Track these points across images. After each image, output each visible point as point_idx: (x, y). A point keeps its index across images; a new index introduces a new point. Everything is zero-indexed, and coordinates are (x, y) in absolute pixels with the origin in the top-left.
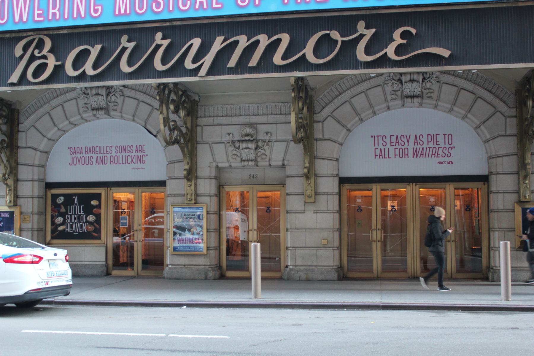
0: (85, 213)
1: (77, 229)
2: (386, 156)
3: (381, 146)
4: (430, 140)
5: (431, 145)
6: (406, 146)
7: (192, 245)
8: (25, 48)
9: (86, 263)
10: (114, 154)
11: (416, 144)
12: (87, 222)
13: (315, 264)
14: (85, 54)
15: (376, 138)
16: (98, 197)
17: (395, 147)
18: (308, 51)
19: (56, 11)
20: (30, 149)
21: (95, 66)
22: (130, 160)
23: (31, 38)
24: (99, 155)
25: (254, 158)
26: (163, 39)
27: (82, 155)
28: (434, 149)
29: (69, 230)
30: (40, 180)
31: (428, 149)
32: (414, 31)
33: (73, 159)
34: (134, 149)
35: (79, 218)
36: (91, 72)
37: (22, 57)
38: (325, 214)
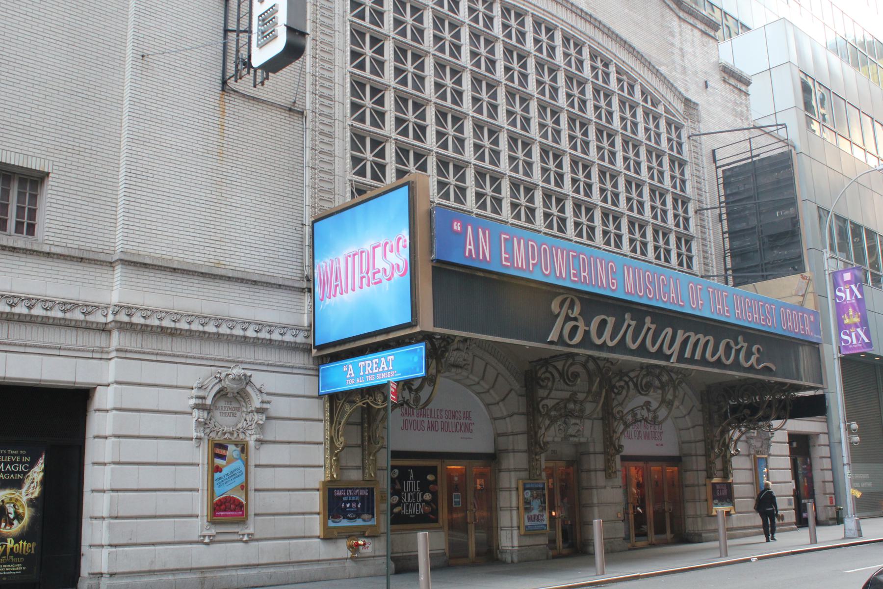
0: (421, 490)
1: (413, 510)
7: (538, 523)
8: (561, 306)
10: (444, 420)
12: (424, 501)
14: (603, 323)
16: (433, 470)
19: (585, 274)
21: (612, 338)
22: (459, 427)
23: (565, 296)
24: (430, 420)
27: (413, 418)
29: (405, 512)
33: (404, 421)
34: (462, 415)
35: (415, 497)
36: (610, 344)
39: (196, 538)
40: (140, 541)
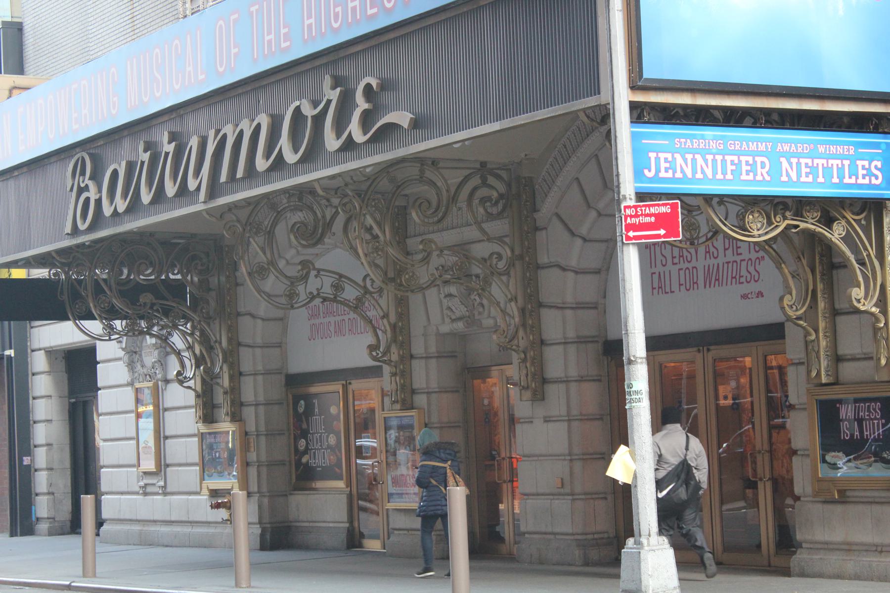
2: (668, 290)
3: (660, 268)
4: (727, 246)
5: (730, 257)
6: (694, 263)
9: (331, 525)
11: (708, 255)
12: (329, 447)
13: (550, 530)
15: (652, 247)
17: (678, 267)
18: (284, 141)
20: (248, 317)
25: (467, 314)
26: (169, 142)
28: (735, 264)
30: (267, 373)
31: (726, 265)
32: (374, 83)
36: (121, 208)
37: (71, 190)
38: (558, 424)
39: (137, 489)
40: (114, 490)
